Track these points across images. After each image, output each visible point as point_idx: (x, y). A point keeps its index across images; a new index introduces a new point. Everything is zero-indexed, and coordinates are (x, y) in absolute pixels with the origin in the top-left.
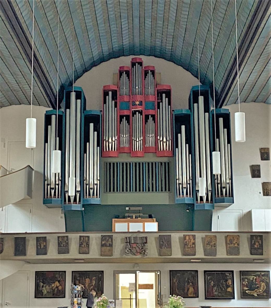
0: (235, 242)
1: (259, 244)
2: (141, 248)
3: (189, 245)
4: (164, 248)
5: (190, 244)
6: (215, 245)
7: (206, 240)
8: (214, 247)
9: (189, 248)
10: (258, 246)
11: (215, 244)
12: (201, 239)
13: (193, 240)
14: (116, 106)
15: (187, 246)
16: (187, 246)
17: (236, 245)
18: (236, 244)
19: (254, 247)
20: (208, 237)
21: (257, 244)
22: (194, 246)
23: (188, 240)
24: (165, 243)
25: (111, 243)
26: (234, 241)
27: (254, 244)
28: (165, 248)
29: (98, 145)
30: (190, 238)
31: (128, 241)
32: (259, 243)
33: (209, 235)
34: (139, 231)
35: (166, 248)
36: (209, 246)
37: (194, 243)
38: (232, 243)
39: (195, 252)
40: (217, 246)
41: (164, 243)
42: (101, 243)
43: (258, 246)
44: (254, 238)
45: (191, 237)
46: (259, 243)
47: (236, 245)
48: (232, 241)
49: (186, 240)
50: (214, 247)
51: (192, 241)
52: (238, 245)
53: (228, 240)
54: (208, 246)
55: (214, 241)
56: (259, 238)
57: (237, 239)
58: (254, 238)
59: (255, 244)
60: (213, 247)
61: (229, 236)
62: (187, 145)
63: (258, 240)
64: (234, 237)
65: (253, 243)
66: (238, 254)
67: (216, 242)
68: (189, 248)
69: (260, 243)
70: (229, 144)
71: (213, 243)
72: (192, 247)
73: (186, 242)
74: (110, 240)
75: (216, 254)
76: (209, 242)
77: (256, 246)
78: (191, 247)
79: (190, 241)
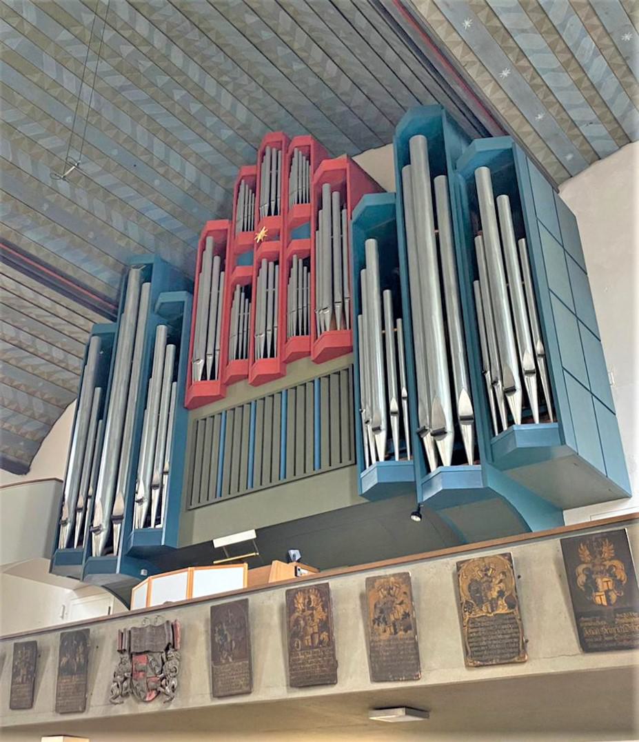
0: (495, 594)
1: (618, 583)
2: (158, 671)
3: (306, 634)
4: (227, 659)
5: (310, 631)
6: (408, 623)
7: (372, 602)
8: (406, 631)
9: (312, 647)
10: (613, 597)
11: (406, 615)
12: (358, 602)
13: (320, 608)
14: (222, 268)
15: (302, 640)
16: (302, 639)
17: (502, 609)
18: (501, 602)
19: (593, 602)
20: (377, 584)
21: (603, 583)
22: (324, 635)
23: (303, 611)
24: (229, 640)
25: (82, 661)
26: (490, 588)
27: (585, 585)
28: (231, 660)
29: (175, 379)
30: (310, 602)
31: (125, 646)
32: (613, 576)
33: (380, 577)
34: (167, 603)
35: (233, 659)
36: (385, 631)
37: (326, 625)
38: (480, 602)
39: (334, 666)
40: (422, 628)
41: (226, 639)
42: (60, 661)
43: (613, 597)
44: (585, 553)
45: (312, 597)
46: (613, 576)
47: (502, 609)
48: (478, 591)
49: (297, 614)
50: (406, 631)
51: (319, 615)
52: (513, 603)
53: (464, 585)
54: (382, 626)
55: (401, 604)
56: (608, 550)
57: (504, 573)
58: (585, 553)
59: (592, 586)
60: (401, 633)
61: (464, 566)
62: (387, 293)
63: (608, 563)
64: (488, 570)
65: (582, 579)
66: (515, 650)
67: (413, 608)
68: (312, 647)
69: (622, 575)
70: (523, 240)
71: (401, 610)
72: (321, 642)
73: (297, 622)
74: (81, 649)
75: (418, 669)
76: (382, 612)
77: (600, 599)
78: (317, 641)
79: (312, 615)
